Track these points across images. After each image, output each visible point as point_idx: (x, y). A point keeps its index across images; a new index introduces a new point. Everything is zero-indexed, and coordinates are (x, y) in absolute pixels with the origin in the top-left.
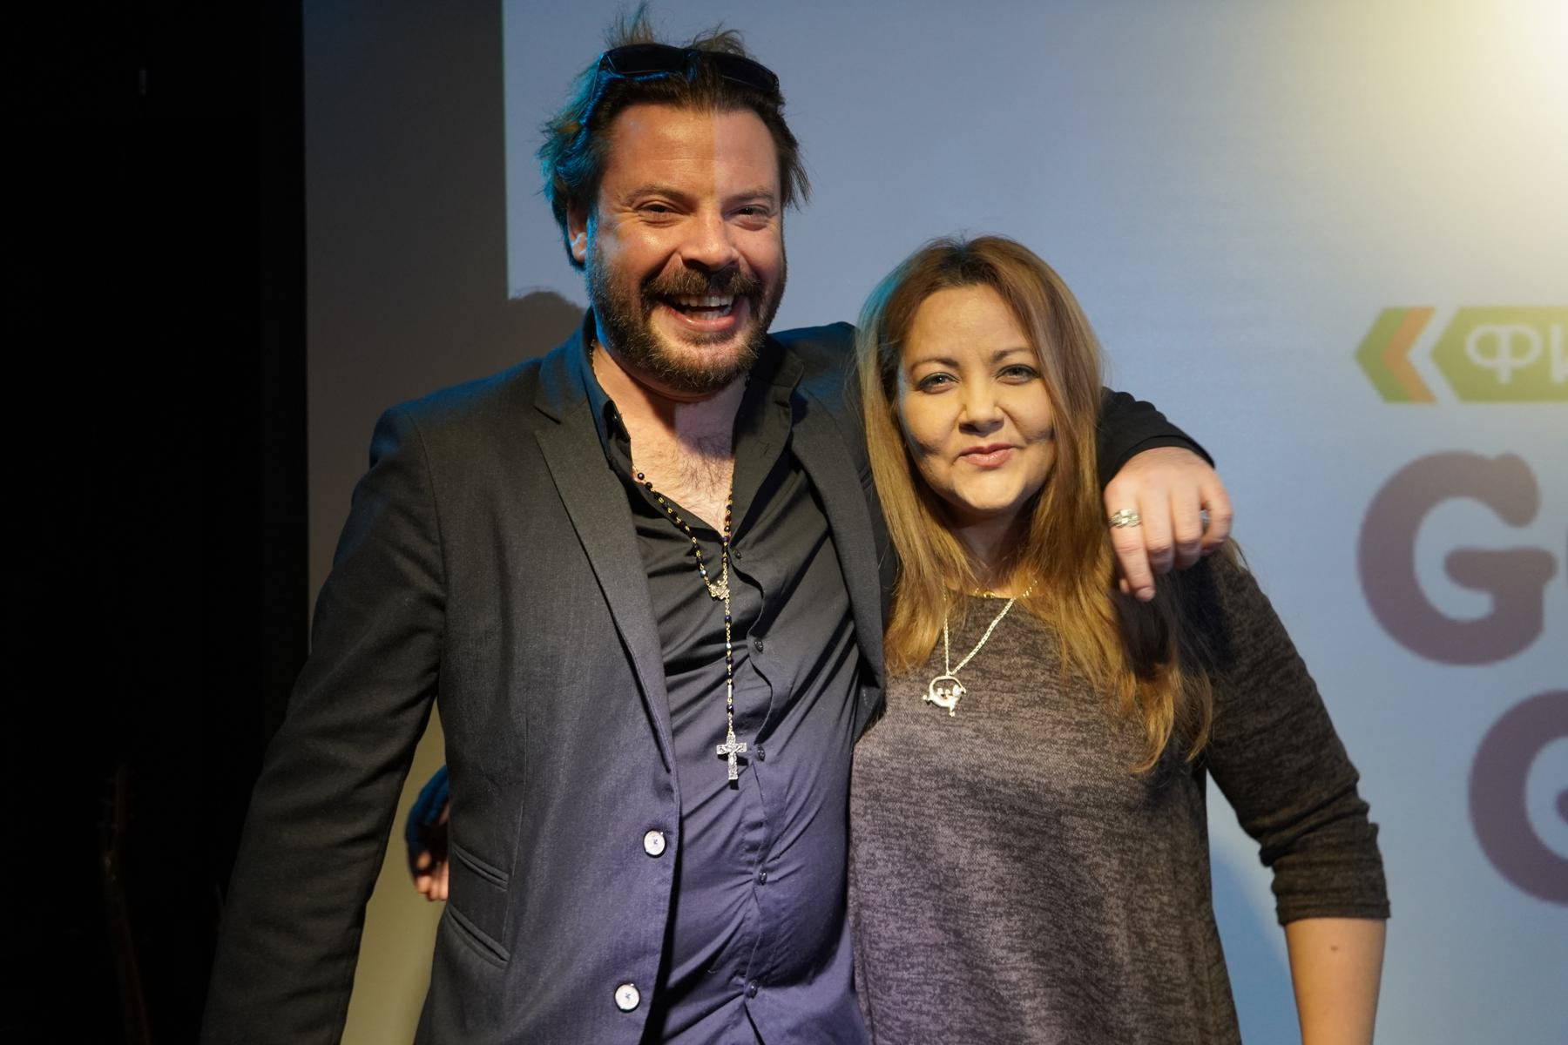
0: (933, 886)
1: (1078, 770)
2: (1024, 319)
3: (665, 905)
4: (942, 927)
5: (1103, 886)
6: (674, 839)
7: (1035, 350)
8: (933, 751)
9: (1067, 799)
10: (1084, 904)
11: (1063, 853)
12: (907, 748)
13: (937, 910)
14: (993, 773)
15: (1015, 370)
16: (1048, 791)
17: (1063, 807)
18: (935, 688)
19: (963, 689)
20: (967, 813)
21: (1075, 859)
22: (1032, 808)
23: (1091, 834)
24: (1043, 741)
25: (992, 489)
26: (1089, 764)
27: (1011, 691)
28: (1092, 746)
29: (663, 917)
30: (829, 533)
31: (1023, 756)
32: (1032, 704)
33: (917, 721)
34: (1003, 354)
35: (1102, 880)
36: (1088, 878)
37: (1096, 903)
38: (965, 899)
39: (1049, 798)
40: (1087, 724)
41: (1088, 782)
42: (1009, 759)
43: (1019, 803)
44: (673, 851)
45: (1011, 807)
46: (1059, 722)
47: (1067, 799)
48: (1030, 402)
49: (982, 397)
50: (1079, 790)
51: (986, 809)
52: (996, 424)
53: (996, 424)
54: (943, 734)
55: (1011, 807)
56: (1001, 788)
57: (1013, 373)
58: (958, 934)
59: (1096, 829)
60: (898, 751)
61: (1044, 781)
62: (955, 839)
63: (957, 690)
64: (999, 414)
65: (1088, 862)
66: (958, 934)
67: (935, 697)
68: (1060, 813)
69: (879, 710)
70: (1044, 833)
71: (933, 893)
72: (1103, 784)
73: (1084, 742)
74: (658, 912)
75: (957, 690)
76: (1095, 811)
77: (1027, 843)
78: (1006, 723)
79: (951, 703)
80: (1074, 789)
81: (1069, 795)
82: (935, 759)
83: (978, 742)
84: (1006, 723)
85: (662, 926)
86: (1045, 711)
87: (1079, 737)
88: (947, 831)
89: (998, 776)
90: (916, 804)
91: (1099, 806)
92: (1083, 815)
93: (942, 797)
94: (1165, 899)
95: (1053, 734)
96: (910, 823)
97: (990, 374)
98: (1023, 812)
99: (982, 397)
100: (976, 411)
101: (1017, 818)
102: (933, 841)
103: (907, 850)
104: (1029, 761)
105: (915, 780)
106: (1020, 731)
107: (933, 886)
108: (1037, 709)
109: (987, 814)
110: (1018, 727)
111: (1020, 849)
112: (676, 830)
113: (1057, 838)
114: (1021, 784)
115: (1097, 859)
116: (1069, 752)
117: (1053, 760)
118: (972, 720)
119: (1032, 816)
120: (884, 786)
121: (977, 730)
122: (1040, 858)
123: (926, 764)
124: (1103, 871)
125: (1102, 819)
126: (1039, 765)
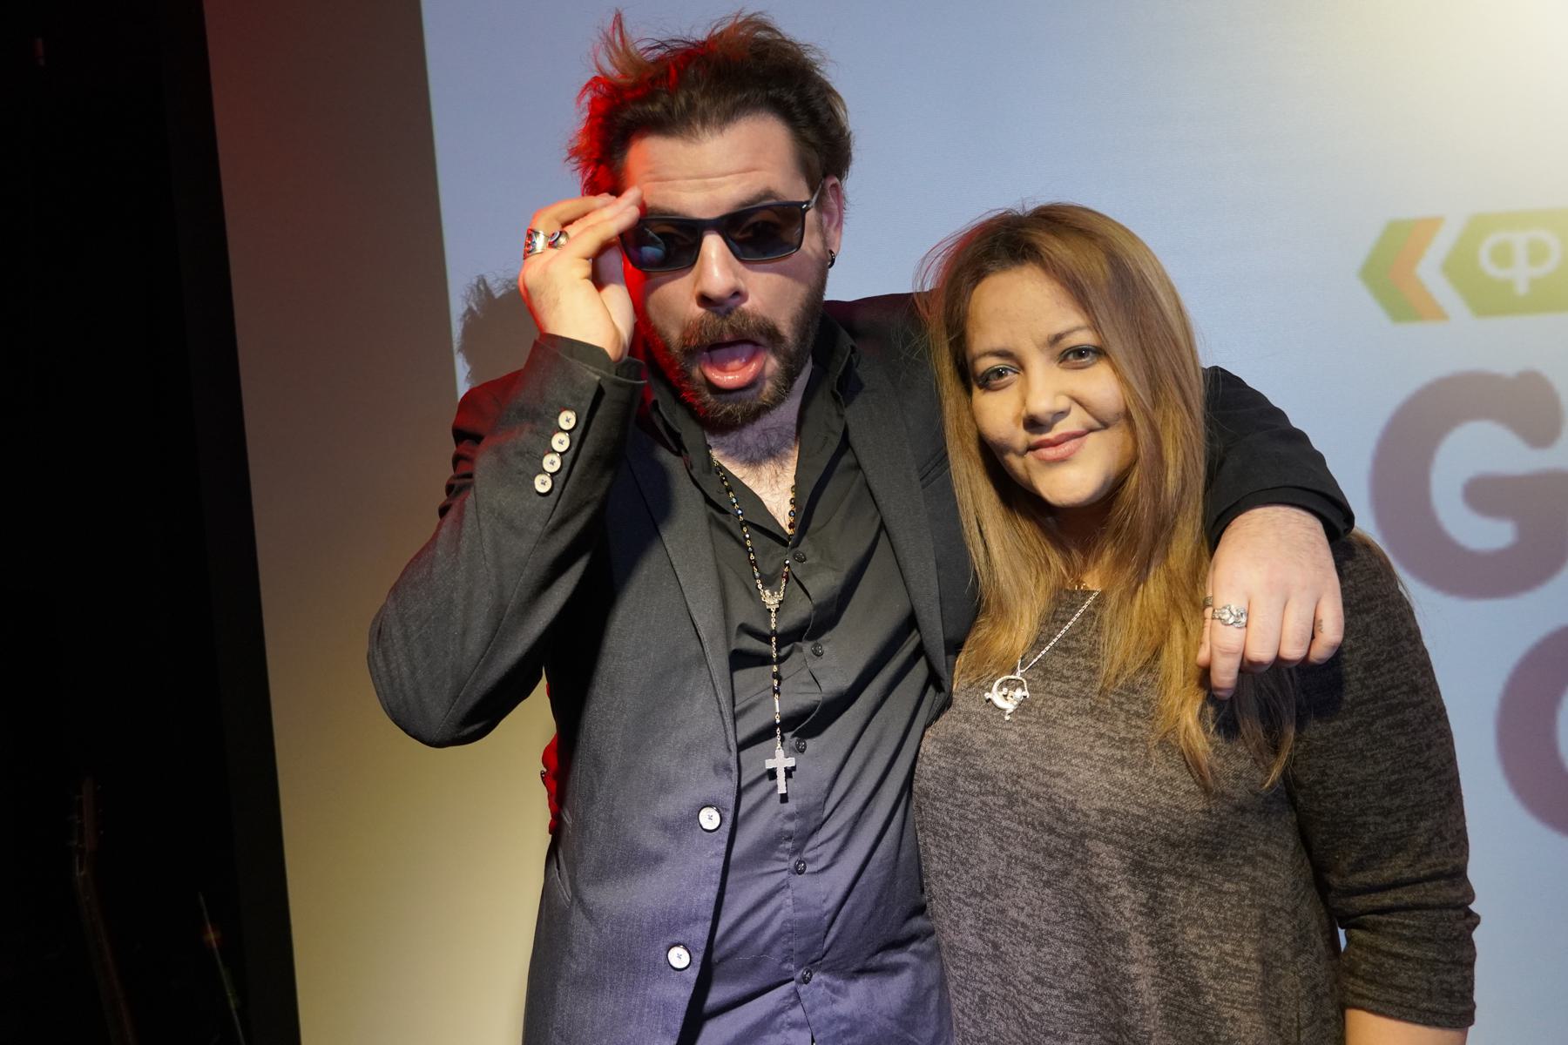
0: (974, 894)
3: (717, 877)
4: (981, 937)
5: (1127, 920)
6: (729, 817)
8: (979, 753)
9: (1091, 820)
10: (1109, 940)
11: (1089, 880)
12: (956, 747)
13: (978, 919)
14: (1028, 785)
15: (1079, 352)
16: (1073, 809)
17: (1088, 828)
19: (1026, 693)
20: (1004, 823)
21: (1099, 889)
22: (1059, 826)
23: (1117, 863)
24: (1081, 754)
25: (1072, 480)
26: (1122, 786)
27: (1066, 696)
28: (1131, 767)
29: (715, 888)
30: (882, 526)
31: (1055, 769)
32: (1080, 713)
33: (967, 720)
35: (1127, 914)
36: (1112, 911)
37: (1122, 940)
38: (1002, 911)
39: (1073, 817)
40: (1132, 742)
41: (1118, 806)
42: (1043, 770)
43: (1047, 819)
44: (727, 827)
45: (1041, 824)
46: (1101, 736)
47: (1091, 820)
48: (1100, 385)
49: (1046, 386)
51: (1020, 823)
52: (1063, 414)
53: (1063, 414)
54: (991, 737)
55: (1041, 824)
56: (1034, 802)
57: (1072, 357)
58: (996, 946)
59: (1123, 858)
60: (946, 749)
61: (1070, 798)
62: (995, 849)
63: (1019, 694)
64: (1062, 403)
65: (1113, 894)
66: (996, 946)
67: (996, 697)
68: (1084, 835)
69: (947, 704)
70: (1071, 856)
71: (974, 901)
72: (1135, 810)
73: (1122, 761)
74: (711, 882)
75: (1019, 694)
76: (1123, 839)
77: (1055, 866)
78: (1050, 731)
79: (1009, 706)
80: (1101, 811)
81: (1094, 816)
82: (980, 763)
83: (1021, 749)
84: (1050, 731)
85: (714, 896)
86: (1090, 721)
87: (1118, 754)
88: (989, 840)
89: (1034, 788)
90: (960, 806)
91: (1130, 835)
92: (1108, 842)
93: (984, 803)
94: (1228, 947)
95: (1092, 748)
96: (954, 825)
97: (1052, 358)
98: (1051, 831)
99: (1046, 386)
100: (1054, 398)
101: (1046, 837)
102: (976, 847)
103: (953, 852)
104: (1060, 775)
105: (960, 781)
106: (1060, 740)
107: (974, 894)
108: (1083, 719)
109: (1021, 829)
110: (1062, 737)
111: (1051, 873)
112: (731, 807)
113: (1083, 863)
114: (1050, 799)
115: (1122, 891)
116: (1103, 770)
117: (1085, 775)
118: (1023, 724)
119: (1059, 836)
120: (931, 784)
121: (1022, 735)
122: (1068, 884)
123: (972, 766)
124: (1128, 904)
125: (1131, 848)
126: (1068, 780)
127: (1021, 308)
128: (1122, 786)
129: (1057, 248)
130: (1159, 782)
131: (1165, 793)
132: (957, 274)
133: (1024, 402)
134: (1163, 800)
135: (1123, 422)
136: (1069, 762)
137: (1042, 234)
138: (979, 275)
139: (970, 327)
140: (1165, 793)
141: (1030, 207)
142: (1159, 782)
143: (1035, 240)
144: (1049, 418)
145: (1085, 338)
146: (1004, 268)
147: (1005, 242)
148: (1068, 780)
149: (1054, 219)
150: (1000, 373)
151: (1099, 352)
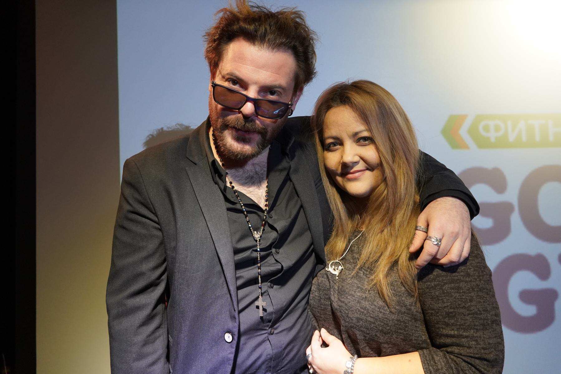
1: (359, 311)
2: (364, 117)
7: (370, 130)
15: (365, 139)
16: (348, 316)
18: (331, 267)
19: (343, 267)
28: (368, 301)
34: (356, 134)
41: (363, 317)
48: (370, 153)
50: (358, 319)
52: (357, 163)
53: (357, 163)
57: (360, 140)
63: (340, 268)
64: (357, 159)
67: (330, 269)
72: (369, 319)
79: (337, 273)
81: (355, 321)
97: (354, 141)
99: (351, 152)
117: (352, 303)
127: (343, 121)
128: (365, 309)
129: (358, 99)
130: (379, 308)
131: (381, 312)
132: (320, 106)
133: (342, 157)
134: (381, 315)
135: (380, 167)
136: (347, 297)
137: (352, 93)
138: (329, 108)
139: (325, 127)
140: (381, 312)
141: (351, 81)
142: (379, 308)
143: (349, 95)
144: (351, 165)
145: (366, 134)
146: (338, 105)
147: (339, 95)
148: (346, 304)
149: (359, 87)
150: (334, 144)
151: (370, 140)
